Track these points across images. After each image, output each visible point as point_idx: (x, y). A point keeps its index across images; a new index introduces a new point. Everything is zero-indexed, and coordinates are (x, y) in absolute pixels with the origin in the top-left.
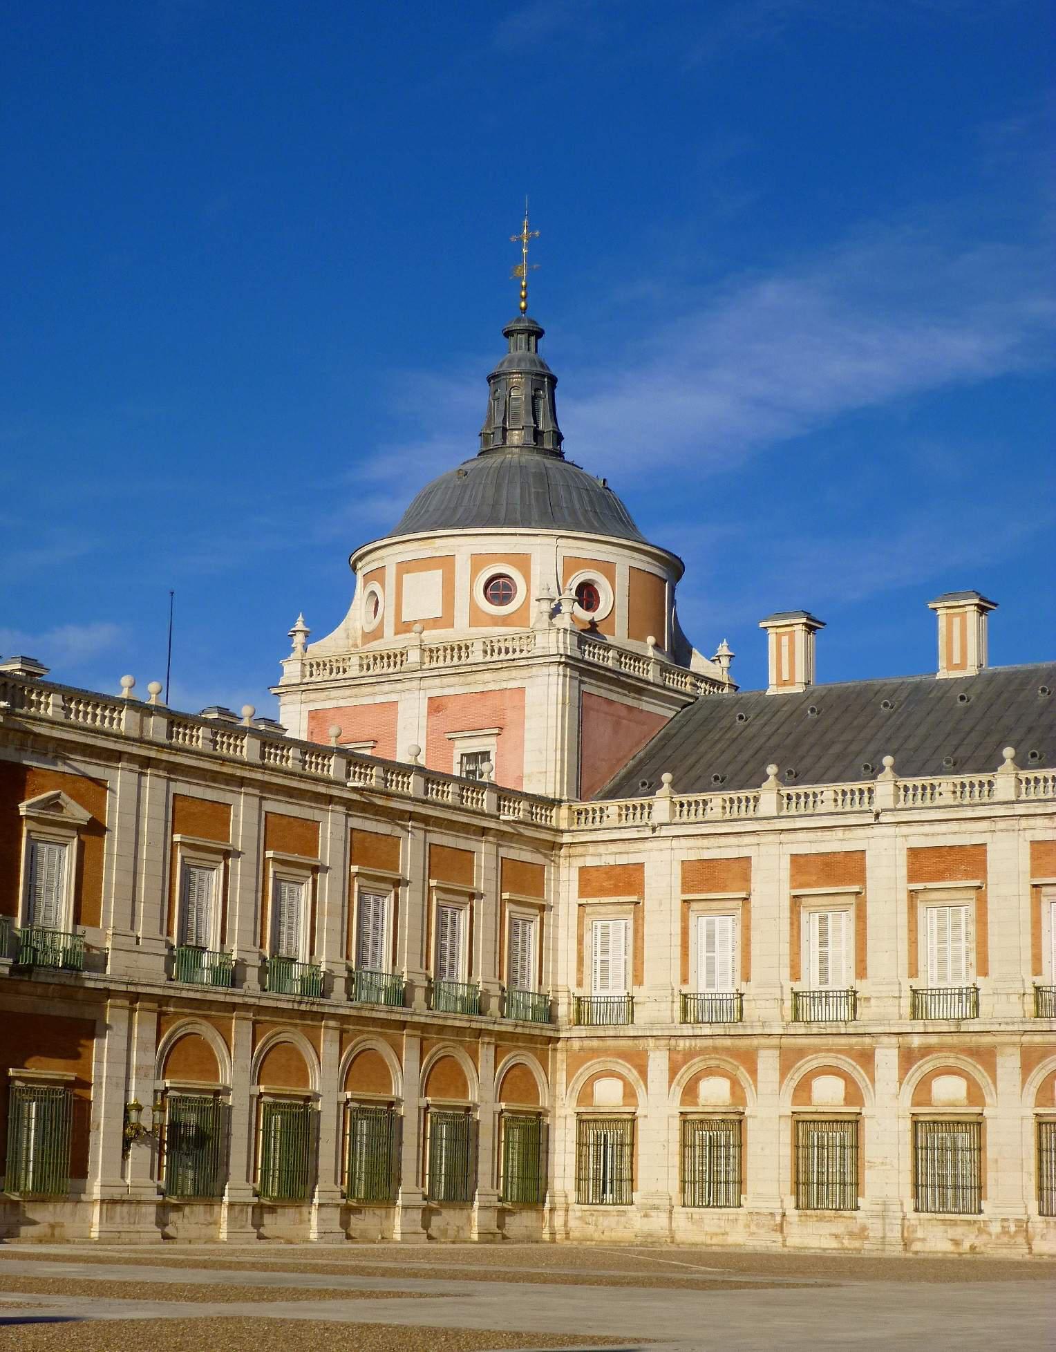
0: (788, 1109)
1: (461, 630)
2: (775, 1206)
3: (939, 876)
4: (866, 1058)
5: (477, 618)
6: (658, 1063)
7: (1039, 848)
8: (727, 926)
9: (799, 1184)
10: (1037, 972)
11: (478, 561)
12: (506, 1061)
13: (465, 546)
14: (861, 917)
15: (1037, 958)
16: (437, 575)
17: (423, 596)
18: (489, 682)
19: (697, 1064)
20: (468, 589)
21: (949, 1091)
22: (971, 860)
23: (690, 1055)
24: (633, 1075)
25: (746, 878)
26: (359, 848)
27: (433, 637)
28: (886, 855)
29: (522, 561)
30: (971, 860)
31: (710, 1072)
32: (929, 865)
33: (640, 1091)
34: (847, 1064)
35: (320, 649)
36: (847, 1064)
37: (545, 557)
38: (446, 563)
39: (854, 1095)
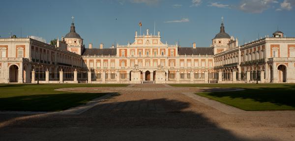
8: (92, 63)
20: (73, 42)
22: (107, 60)
28: (102, 60)
32: (104, 60)
37: (78, 40)
38: (72, 40)
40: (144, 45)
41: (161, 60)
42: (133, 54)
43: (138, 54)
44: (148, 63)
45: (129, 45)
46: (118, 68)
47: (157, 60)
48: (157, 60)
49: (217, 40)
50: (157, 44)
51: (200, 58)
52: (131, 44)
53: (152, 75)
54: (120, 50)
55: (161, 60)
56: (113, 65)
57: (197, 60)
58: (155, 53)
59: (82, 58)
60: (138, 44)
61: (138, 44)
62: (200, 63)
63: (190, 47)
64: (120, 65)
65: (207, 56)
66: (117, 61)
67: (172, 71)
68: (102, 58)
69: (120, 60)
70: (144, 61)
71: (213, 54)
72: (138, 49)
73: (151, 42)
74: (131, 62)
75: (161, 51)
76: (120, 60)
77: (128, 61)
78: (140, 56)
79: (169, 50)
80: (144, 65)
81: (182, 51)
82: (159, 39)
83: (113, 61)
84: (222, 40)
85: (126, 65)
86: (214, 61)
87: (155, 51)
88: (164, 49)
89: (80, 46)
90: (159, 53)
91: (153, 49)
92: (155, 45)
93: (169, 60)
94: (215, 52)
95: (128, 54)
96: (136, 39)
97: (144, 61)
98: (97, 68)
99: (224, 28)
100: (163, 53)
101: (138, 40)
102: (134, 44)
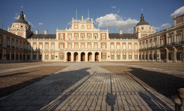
1: (19, 29)
5: (20, 28)
7: (51, 43)
8: (35, 46)
9: (39, 58)
13: (20, 24)
16: (18, 25)
17: (17, 26)
18: (21, 32)
20: (20, 26)
21: (47, 54)
22: (48, 43)
26: (17, 40)
27: (18, 29)
28: (44, 42)
29: (23, 25)
32: (46, 43)
35: (10, 28)
37: (24, 25)
38: (19, 25)
40: (80, 29)
41: (94, 43)
42: (70, 37)
43: (74, 37)
44: (83, 46)
45: (66, 30)
46: (57, 50)
47: (91, 43)
48: (91, 43)
49: (140, 27)
50: (91, 28)
51: (127, 41)
52: (68, 29)
53: (86, 56)
54: (59, 34)
55: (94, 43)
57: (125, 43)
58: (89, 37)
59: (26, 41)
60: (74, 28)
61: (74, 28)
63: (117, 33)
64: (59, 47)
65: (133, 39)
66: (57, 43)
67: (103, 53)
69: (59, 43)
70: (80, 44)
71: (137, 38)
72: (75, 33)
73: (86, 27)
74: (68, 45)
75: (94, 35)
76: (59, 43)
77: (66, 44)
78: (76, 39)
79: (101, 34)
80: (80, 47)
81: (112, 36)
82: (92, 25)
84: (145, 26)
85: (64, 48)
86: (138, 43)
87: (89, 34)
88: (97, 33)
89: (25, 30)
91: (87, 33)
93: (101, 43)
94: (140, 37)
95: (65, 38)
96: (72, 24)
97: (80, 44)
99: (143, 17)
100: (96, 37)
101: (74, 25)
102: (72, 28)
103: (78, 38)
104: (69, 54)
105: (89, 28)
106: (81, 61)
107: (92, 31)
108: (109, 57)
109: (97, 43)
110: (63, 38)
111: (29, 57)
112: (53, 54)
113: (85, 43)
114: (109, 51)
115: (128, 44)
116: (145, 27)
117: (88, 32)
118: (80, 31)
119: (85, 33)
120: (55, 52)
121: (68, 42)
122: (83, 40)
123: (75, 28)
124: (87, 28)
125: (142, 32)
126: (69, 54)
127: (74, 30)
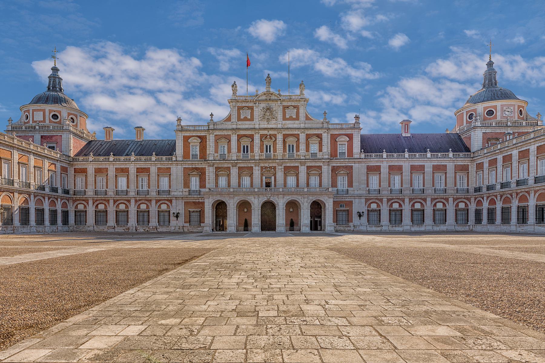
0: (115, 209)
2: (113, 225)
3: (142, 172)
4: (129, 201)
6: (91, 202)
10: (158, 188)
11: (50, 111)
12: (63, 201)
14: (128, 178)
15: (158, 186)
19: (98, 202)
23: (97, 200)
24: (86, 204)
25: (107, 171)
30: (147, 170)
31: (100, 203)
33: (87, 206)
34: (125, 202)
36: (125, 202)
38: (44, 111)
39: (127, 207)
40: (257, 123)
41: (308, 168)
43: (239, 151)
55: (308, 168)
56: (164, 183)
62: (428, 177)
64: (186, 184)
66: (177, 171)
68: (133, 164)
72: (240, 137)
73: (280, 116)
77: (210, 173)
83: (165, 172)
85: (202, 184)
87: (291, 141)
88: (319, 136)
90: (303, 147)
92: (289, 124)
93: (334, 170)
98: (117, 193)
103: (252, 151)
104: (220, 208)
105: (291, 119)
106: (262, 230)
107: (302, 126)
108: (360, 216)
109: (320, 167)
110: (198, 153)
111: (81, 216)
112: (164, 207)
113: (275, 168)
114: (360, 196)
115: (387, 170)
116: (499, 108)
117: (287, 132)
118: (260, 129)
119: (275, 136)
120: (171, 201)
121: (216, 166)
122: (268, 159)
123: (242, 117)
124: (284, 119)
125: (488, 127)
126: (220, 208)
127: (239, 127)
